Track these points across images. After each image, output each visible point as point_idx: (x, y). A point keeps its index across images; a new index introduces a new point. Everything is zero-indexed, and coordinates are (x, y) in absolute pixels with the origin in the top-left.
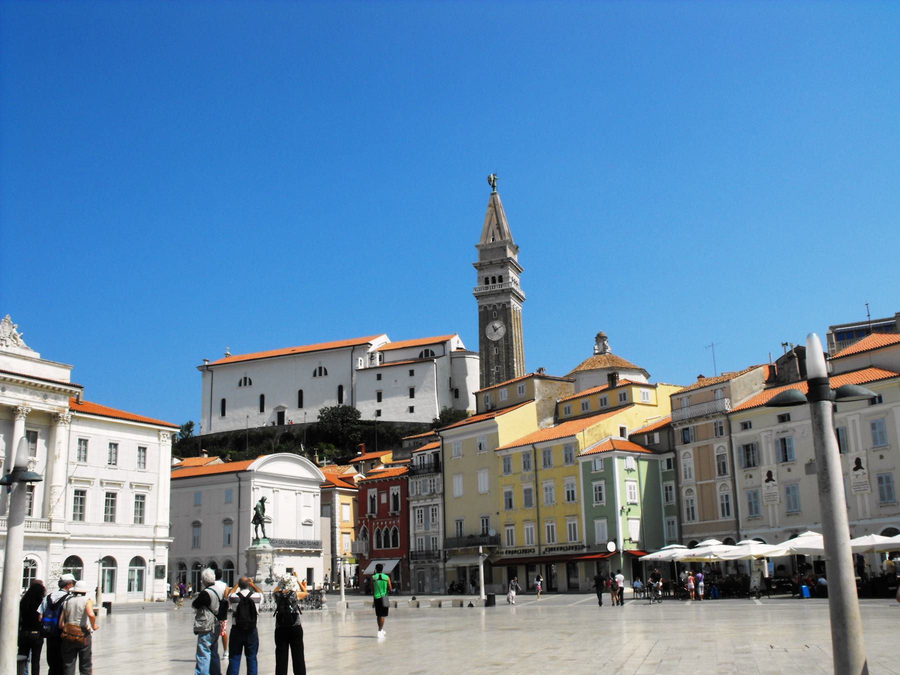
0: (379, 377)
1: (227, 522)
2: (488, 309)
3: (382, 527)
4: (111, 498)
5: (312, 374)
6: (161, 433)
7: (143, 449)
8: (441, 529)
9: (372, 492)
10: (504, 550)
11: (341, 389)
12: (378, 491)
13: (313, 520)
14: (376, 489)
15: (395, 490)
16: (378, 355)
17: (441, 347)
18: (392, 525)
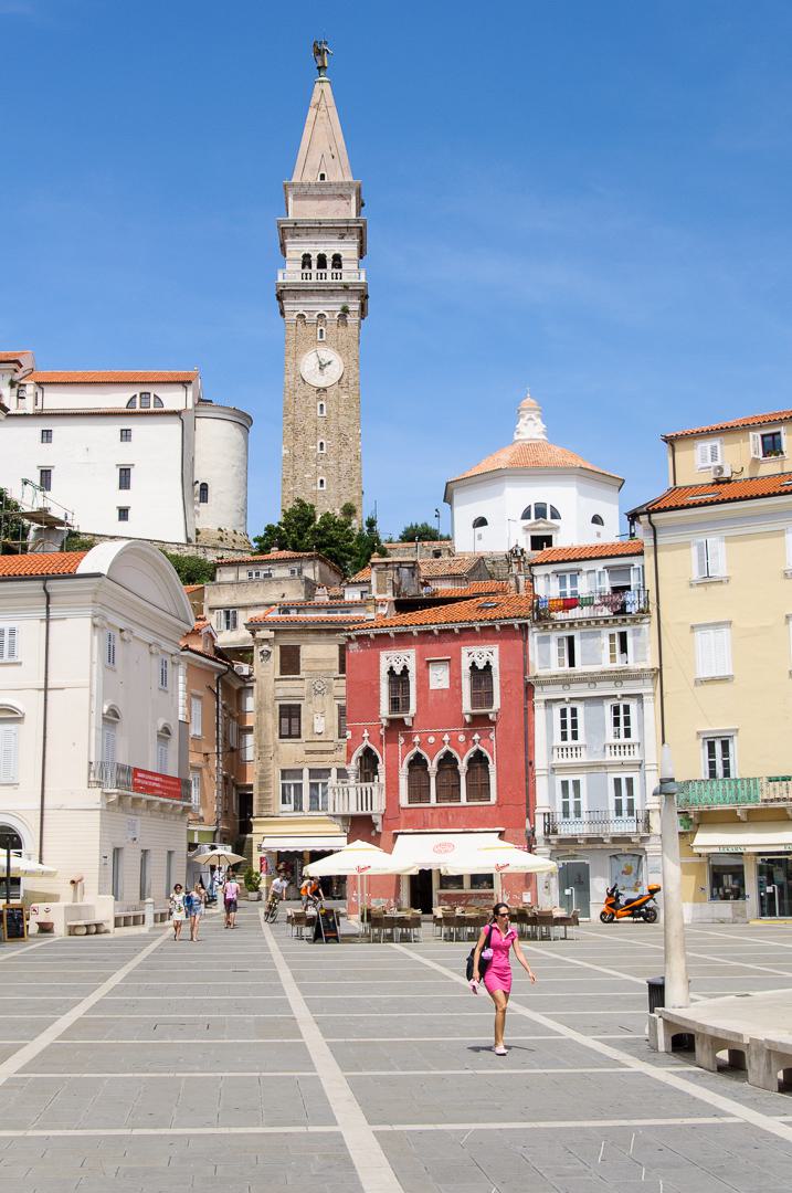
3: (433, 750)
12: (420, 657)
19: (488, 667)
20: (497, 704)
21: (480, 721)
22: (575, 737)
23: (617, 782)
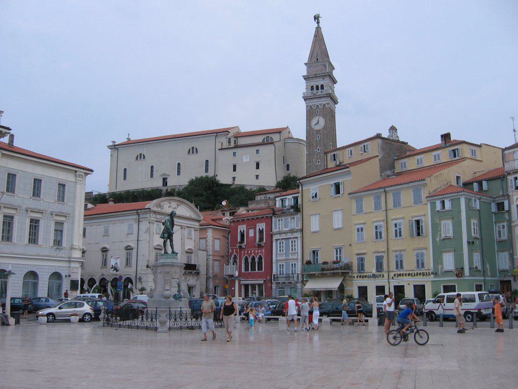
0: (234, 154)
1: (129, 248)
2: (314, 108)
4: (34, 224)
5: (187, 152)
6: (78, 173)
7: (62, 186)
8: (300, 257)
9: (242, 228)
10: (356, 275)
11: (207, 161)
12: (247, 227)
13: (193, 248)
14: (245, 226)
15: (262, 226)
16: (233, 140)
17: (278, 135)
18: (258, 253)
19: (263, 229)
20: (264, 241)
21: (260, 246)
22: (283, 251)
23: (292, 264)
